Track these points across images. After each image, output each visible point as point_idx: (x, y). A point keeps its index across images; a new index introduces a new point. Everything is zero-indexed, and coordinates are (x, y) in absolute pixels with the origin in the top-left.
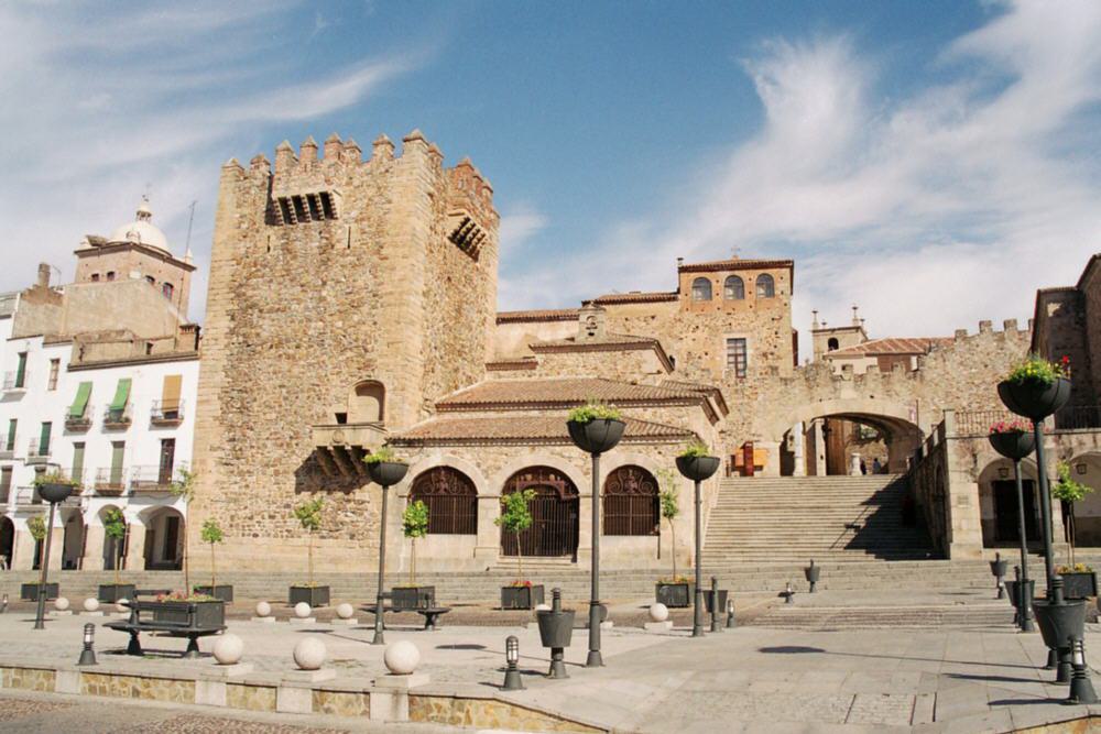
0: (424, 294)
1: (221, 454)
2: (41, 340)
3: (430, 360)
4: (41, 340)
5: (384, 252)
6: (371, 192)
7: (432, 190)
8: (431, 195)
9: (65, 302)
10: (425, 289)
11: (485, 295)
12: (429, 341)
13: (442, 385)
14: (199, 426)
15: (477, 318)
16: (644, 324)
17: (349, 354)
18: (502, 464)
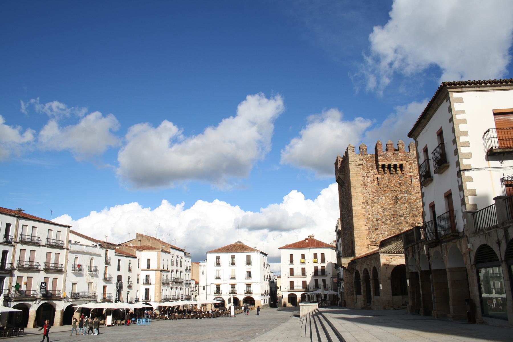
0: (363, 203)
3: (373, 226)
7: (361, 162)
10: (364, 201)
12: (371, 219)
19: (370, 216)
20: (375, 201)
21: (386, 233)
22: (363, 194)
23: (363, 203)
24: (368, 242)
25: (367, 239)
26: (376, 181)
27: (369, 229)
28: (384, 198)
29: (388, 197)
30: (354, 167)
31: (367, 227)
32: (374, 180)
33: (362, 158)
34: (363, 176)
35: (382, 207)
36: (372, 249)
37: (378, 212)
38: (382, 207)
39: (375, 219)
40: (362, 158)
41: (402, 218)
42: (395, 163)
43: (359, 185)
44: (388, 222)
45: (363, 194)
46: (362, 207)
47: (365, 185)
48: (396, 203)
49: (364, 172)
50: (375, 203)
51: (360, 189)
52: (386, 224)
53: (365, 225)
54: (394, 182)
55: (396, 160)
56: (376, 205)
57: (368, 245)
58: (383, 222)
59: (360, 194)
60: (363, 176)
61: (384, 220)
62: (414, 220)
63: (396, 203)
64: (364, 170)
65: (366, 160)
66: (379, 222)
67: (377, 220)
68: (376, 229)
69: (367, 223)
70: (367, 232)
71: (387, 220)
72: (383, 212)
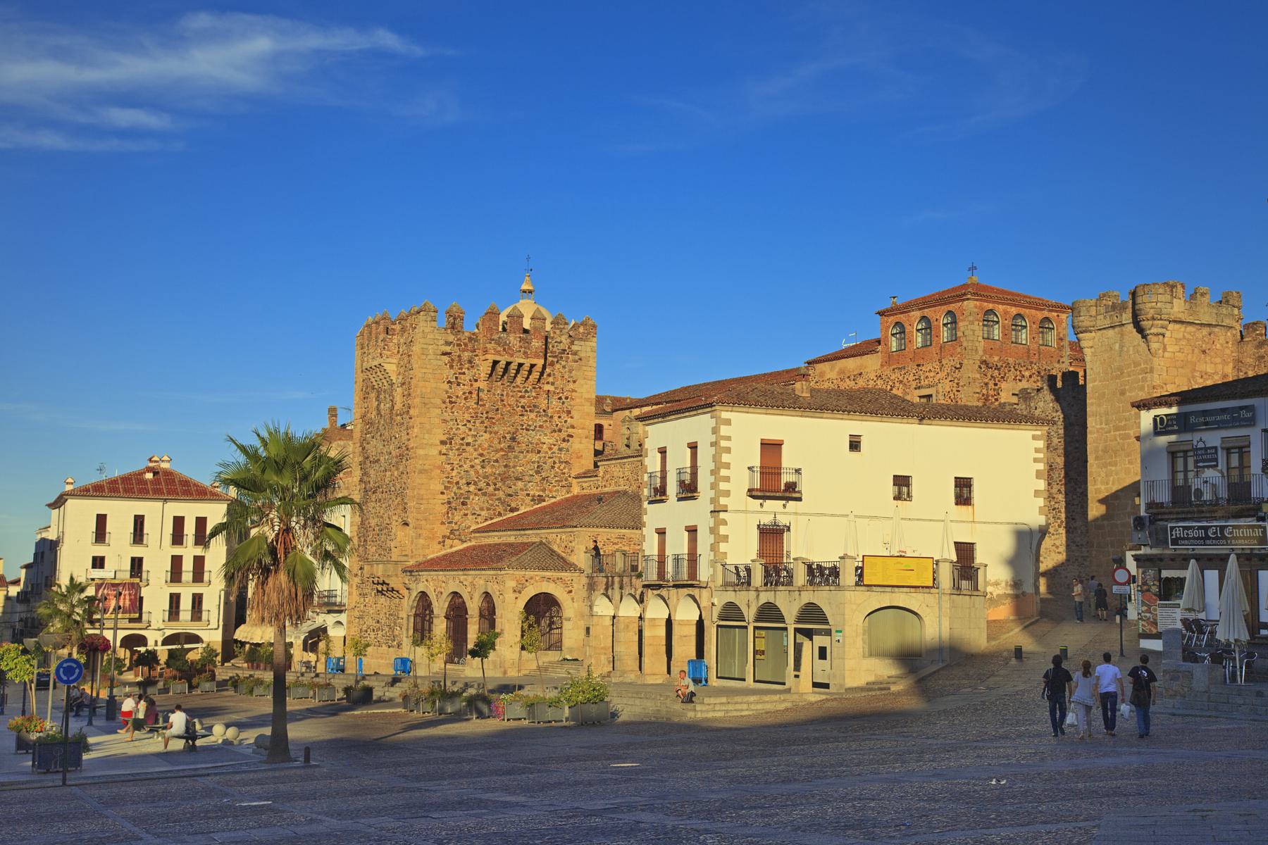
0: (443, 443)
7: (448, 349)
10: (444, 438)
12: (455, 480)
19: (454, 473)
20: (470, 440)
23: (443, 443)
27: (449, 503)
37: (472, 467)
40: (451, 338)
42: (521, 361)
43: (439, 401)
44: (491, 488)
47: (451, 402)
50: (468, 444)
55: (525, 353)
57: (444, 537)
59: (437, 421)
65: (459, 345)
66: (472, 488)
67: (468, 484)
69: (446, 488)
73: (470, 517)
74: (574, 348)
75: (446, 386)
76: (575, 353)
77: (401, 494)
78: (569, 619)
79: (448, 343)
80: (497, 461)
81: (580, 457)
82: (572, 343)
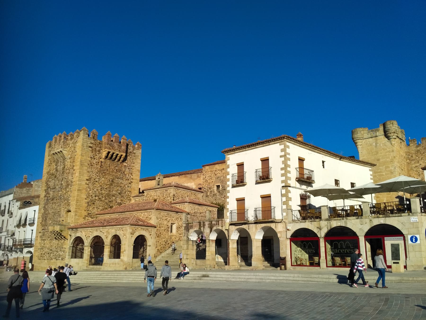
0: (87, 180)
1: (40, 234)
2: (16, 200)
3: (91, 201)
4: (16, 200)
5: (74, 168)
6: (73, 149)
7: (91, 145)
8: (90, 147)
9: (34, 186)
10: (88, 178)
11: (132, 174)
12: (91, 194)
13: (100, 208)
14: (37, 226)
15: (125, 182)
16: (220, 172)
17: (66, 201)
18: (90, 235)
19: (91, 192)
20: (97, 180)
21: (100, 208)
22: (88, 172)
23: (87, 180)
24: (85, 213)
25: (85, 211)
26: (100, 164)
27: (88, 203)
28: (103, 179)
29: (107, 178)
30: (85, 147)
31: (87, 200)
32: (98, 163)
33: (93, 142)
34: (91, 158)
35: (101, 186)
36: (88, 220)
37: (97, 190)
38: (101, 186)
39: (94, 195)
40: (93, 142)
41: (114, 198)
42: (118, 153)
43: (86, 164)
44: (104, 199)
45: (88, 172)
46: (86, 184)
47: (91, 165)
48: (111, 184)
49: (92, 154)
50: (96, 181)
51: (87, 168)
52: (101, 201)
53: (86, 199)
54: (113, 167)
55: (119, 150)
56: (97, 183)
57: (85, 216)
58: (100, 199)
59: (86, 171)
60: (91, 158)
61: (100, 197)
62: (122, 201)
63: (111, 184)
64: (92, 152)
65: (95, 145)
66: (97, 198)
67: (96, 196)
68: (93, 204)
69: (87, 197)
70: (86, 205)
71: (103, 197)
72: (101, 190)
73: (95, 209)
74: (134, 152)
75: (90, 159)
76: (134, 153)
77: (68, 200)
78: (150, 246)
79: (92, 143)
80: (106, 189)
81: (135, 190)
82: (134, 150)
